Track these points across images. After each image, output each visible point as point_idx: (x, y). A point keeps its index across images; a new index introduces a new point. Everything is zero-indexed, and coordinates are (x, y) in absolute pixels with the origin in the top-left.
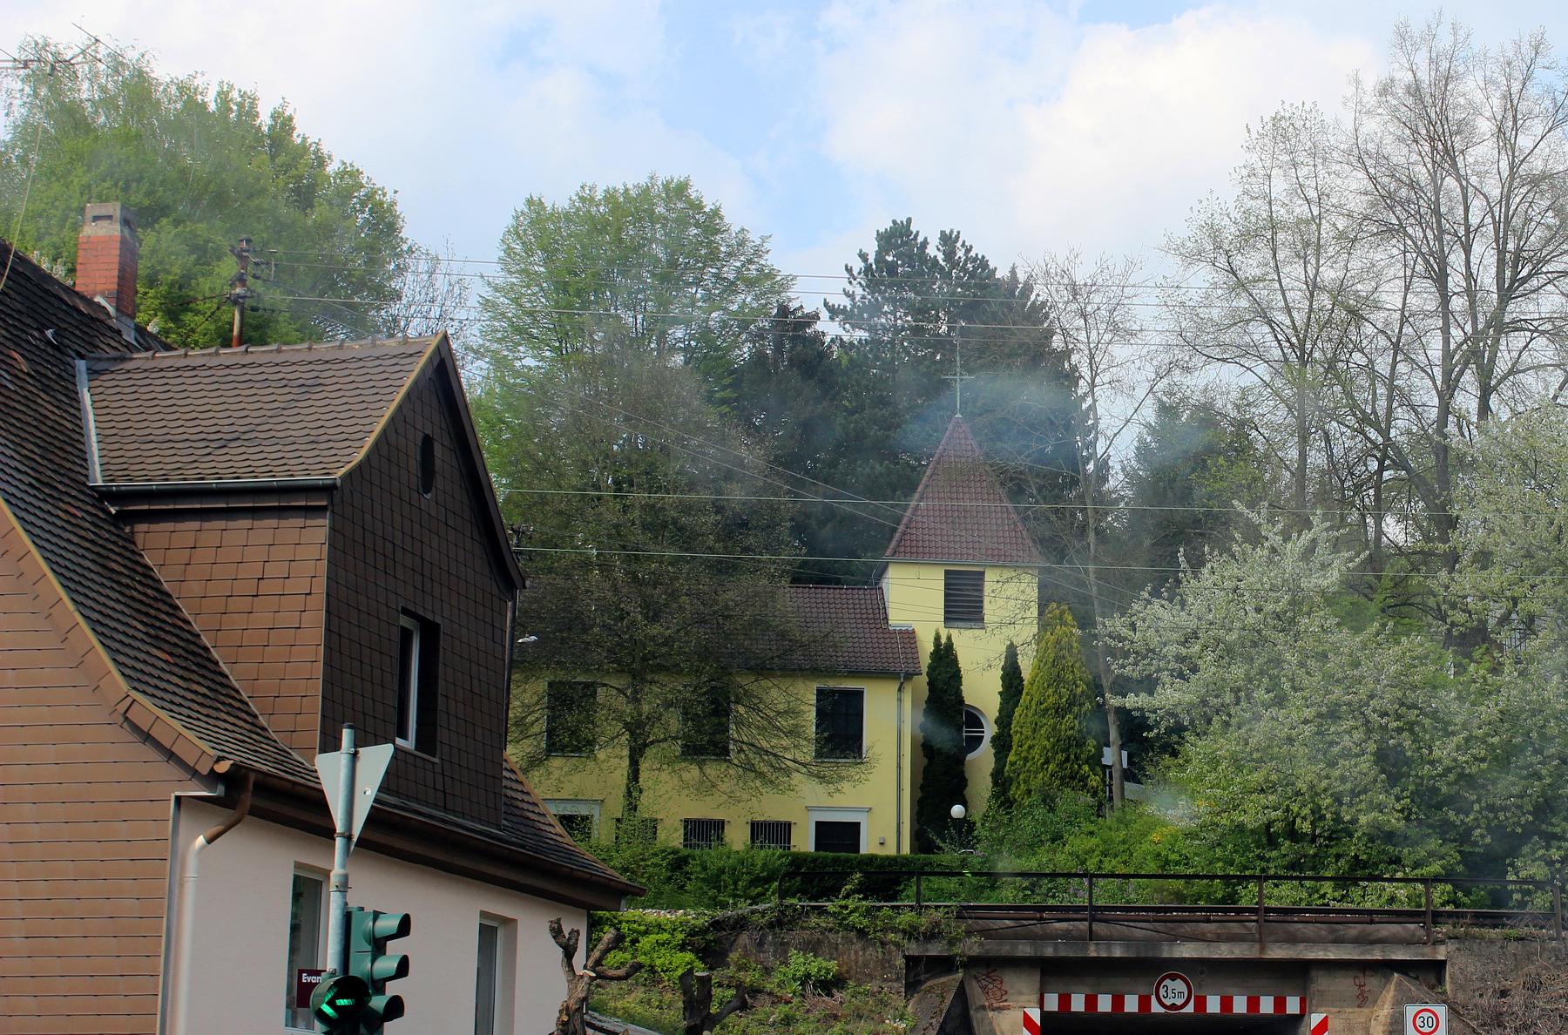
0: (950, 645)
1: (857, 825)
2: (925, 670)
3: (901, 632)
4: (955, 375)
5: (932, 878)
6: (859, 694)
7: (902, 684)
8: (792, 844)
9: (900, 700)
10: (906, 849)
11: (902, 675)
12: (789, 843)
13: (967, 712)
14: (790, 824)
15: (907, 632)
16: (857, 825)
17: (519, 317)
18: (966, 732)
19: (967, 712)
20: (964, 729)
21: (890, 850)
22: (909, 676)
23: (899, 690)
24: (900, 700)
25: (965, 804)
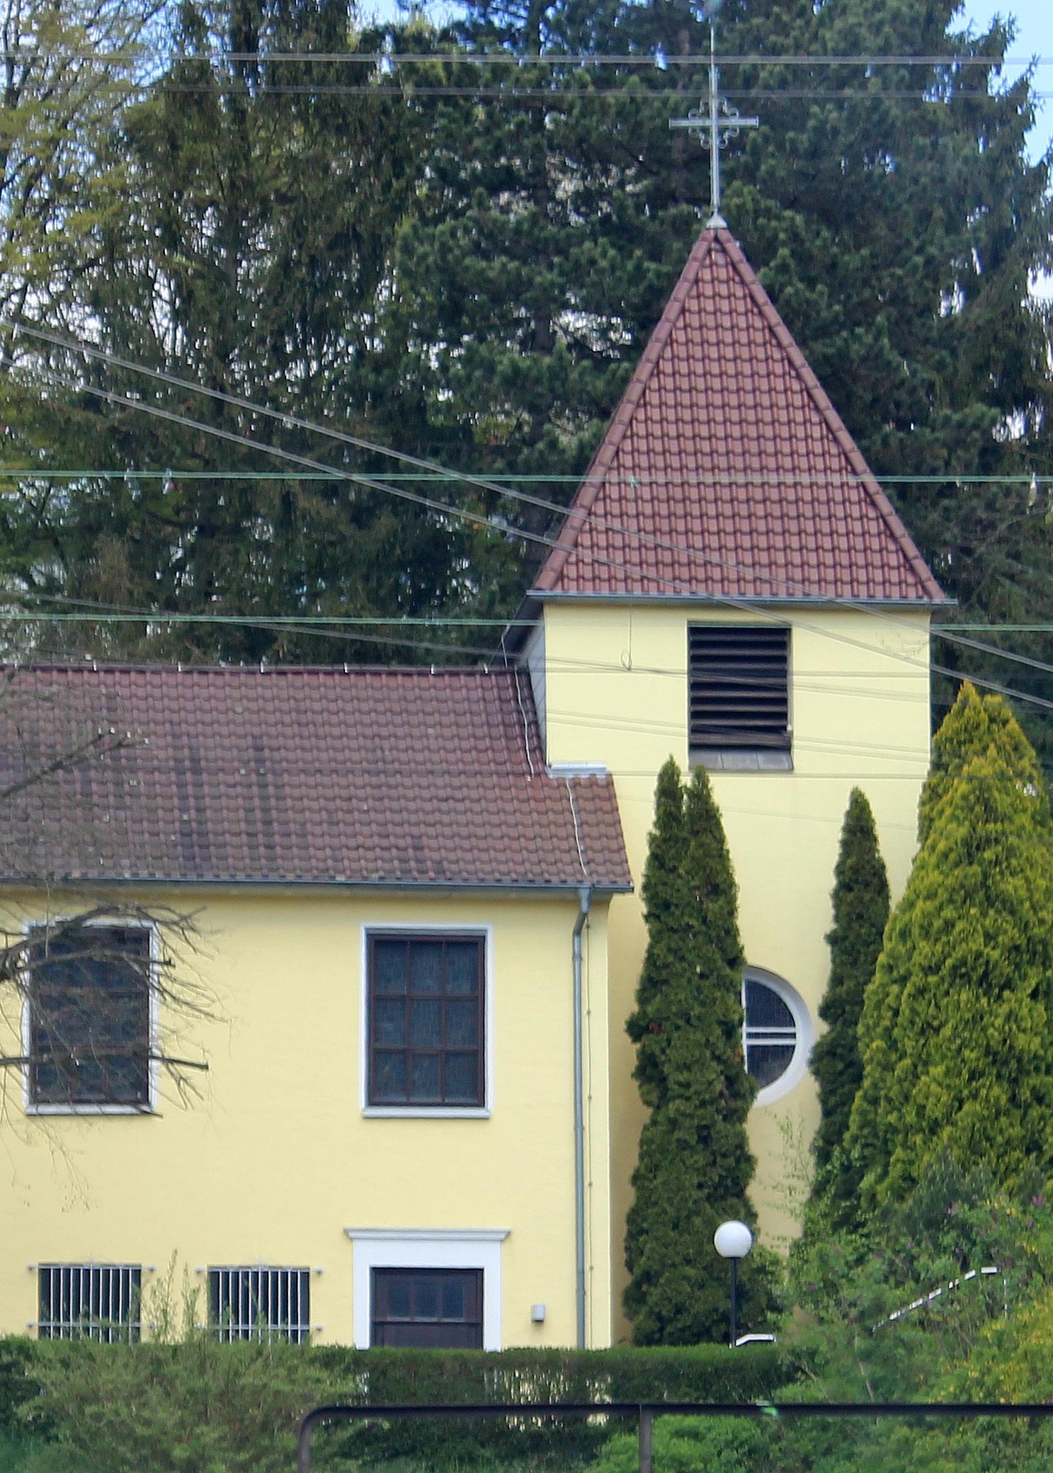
0: (701, 794)
1: (476, 1275)
2: (638, 880)
3: (576, 784)
4: (706, 131)
5: (873, 1399)
6: (473, 946)
7: (584, 916)
8: (314, 1323)
9: (577, 957)
10: (601, 1337)
11: (584, 894)
12: (306, 1320)
13: (753, 988)
14: (306, 1275)
15: (592, 783)
16: (476, 1275)
17: (189, 1025)
18: (750, 1035)
19: (753, 988)
20: (745, 1029)
21: (560, 1336)
22: (600, 898)
23: (578, 932)
24: (577, 957)
25: (750, 1218)
